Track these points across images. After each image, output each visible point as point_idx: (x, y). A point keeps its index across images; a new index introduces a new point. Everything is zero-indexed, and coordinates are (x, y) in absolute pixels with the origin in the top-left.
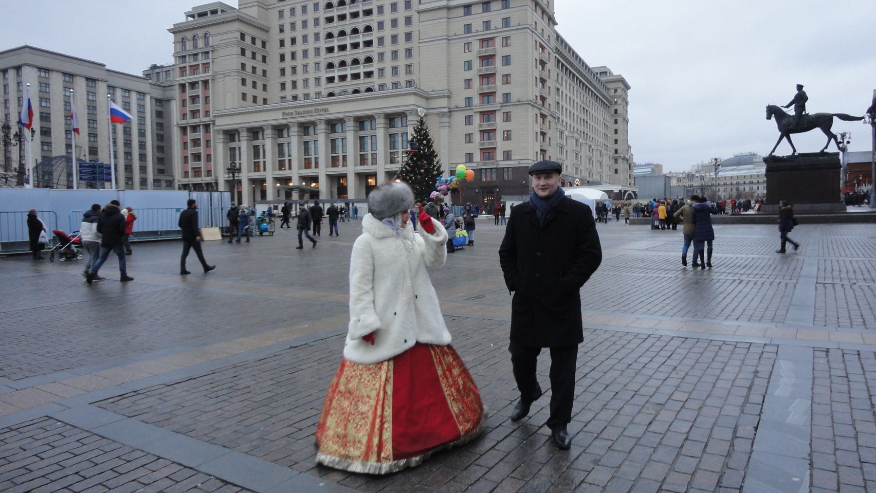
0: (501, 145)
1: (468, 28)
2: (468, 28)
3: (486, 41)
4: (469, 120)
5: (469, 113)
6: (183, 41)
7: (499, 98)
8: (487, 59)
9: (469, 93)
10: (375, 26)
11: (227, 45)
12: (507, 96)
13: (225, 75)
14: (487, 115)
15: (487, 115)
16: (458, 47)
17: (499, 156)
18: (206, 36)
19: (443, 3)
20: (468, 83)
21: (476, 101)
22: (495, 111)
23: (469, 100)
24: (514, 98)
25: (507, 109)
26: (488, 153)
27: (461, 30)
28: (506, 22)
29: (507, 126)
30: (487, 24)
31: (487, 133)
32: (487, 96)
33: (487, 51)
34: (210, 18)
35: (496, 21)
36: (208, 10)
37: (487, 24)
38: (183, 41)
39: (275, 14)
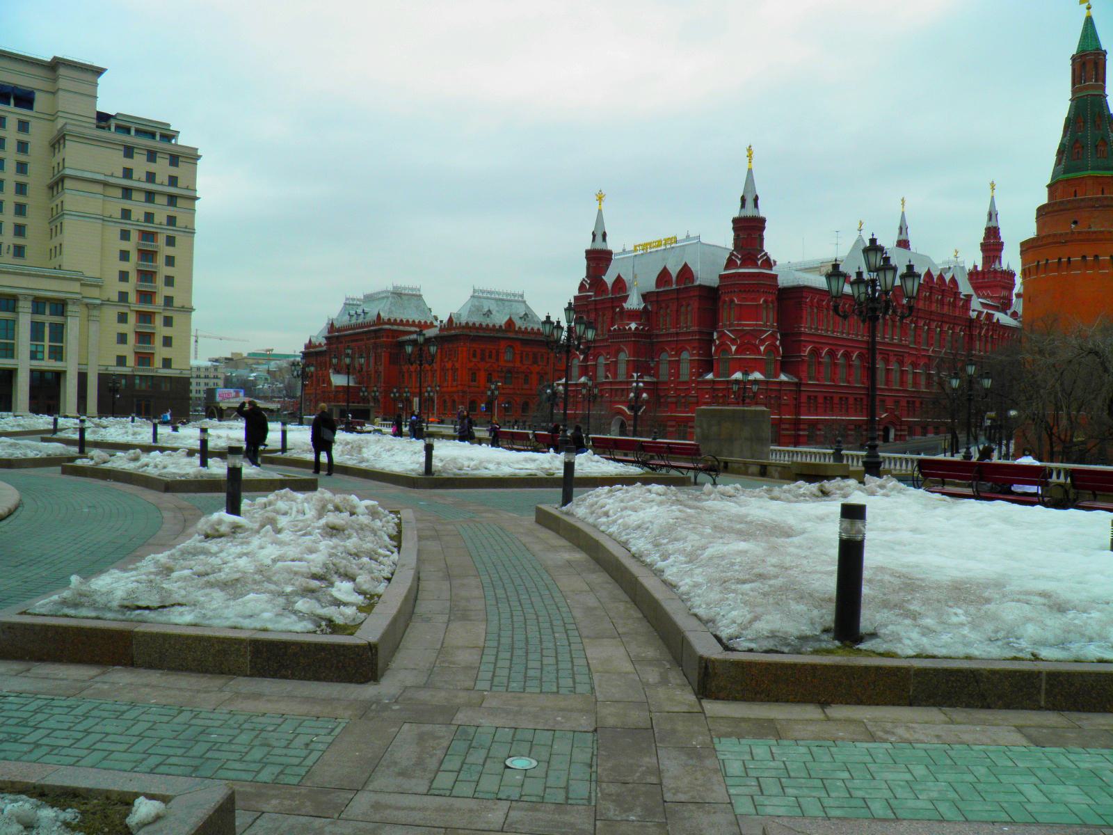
0: (160, 352)
1: (126, 214)
2: (126, 214)
3: (148, 236)
4: (122, 318)
5: (124, 310)
7: (160, 300)
8: (148, 255)
9: (124, 287)
12: (169, 301)
14: (146, 317)
15: (146, 317)
16: (115, 232)
17: (158, 362)
19: (101, 177)
20: (124, 276)
21: (132, 298)
22: (154, 313)
23: (123, 296)
24: (177, 303)
25: (168, 314)
26: (144, 358)
27: (118, 214)
28: (171, 220)
30: (149, 217)
31: (144, 337)
32: (146, 296)
35: (161, 215)
37: (149, 217)
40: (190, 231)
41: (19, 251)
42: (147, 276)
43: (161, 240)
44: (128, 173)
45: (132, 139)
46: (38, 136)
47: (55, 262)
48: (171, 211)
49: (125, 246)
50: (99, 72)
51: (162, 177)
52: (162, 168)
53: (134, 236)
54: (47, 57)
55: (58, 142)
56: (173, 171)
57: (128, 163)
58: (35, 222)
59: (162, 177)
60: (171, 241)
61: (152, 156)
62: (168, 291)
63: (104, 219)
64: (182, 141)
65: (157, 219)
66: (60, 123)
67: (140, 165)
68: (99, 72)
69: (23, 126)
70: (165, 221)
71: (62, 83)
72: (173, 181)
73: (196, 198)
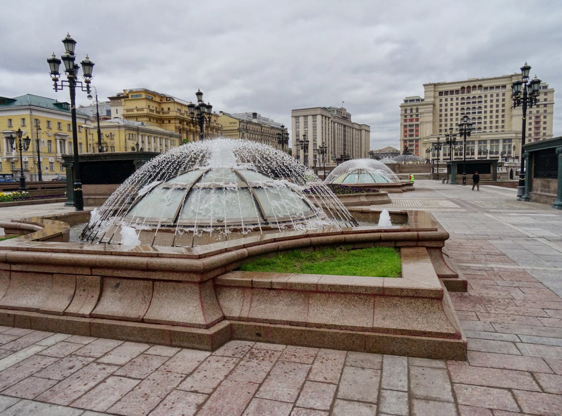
3: (537, 117)
6: (406, 110)
11: (428, 112)
12: (544, 134)
13: (427, 123)
18: (417, 109)
21: (533, 135)
24: (547, 134)
30: (538, 112)
33: (538, 120)
34: (420, 103)
38: (406, 110)
39: (438, 100)
40: (552, 113)
41: (503, 127)
42: (537, 128)
43: (542, 117)
48: (545, 109)
53: (533, 118)
56: (545, 97)
58: (506, 118)
60: (545, 117)
62: (545, 131)
64: (549, 87)
69: (504, 95)
70: (543, 112)
73: (553, 103)
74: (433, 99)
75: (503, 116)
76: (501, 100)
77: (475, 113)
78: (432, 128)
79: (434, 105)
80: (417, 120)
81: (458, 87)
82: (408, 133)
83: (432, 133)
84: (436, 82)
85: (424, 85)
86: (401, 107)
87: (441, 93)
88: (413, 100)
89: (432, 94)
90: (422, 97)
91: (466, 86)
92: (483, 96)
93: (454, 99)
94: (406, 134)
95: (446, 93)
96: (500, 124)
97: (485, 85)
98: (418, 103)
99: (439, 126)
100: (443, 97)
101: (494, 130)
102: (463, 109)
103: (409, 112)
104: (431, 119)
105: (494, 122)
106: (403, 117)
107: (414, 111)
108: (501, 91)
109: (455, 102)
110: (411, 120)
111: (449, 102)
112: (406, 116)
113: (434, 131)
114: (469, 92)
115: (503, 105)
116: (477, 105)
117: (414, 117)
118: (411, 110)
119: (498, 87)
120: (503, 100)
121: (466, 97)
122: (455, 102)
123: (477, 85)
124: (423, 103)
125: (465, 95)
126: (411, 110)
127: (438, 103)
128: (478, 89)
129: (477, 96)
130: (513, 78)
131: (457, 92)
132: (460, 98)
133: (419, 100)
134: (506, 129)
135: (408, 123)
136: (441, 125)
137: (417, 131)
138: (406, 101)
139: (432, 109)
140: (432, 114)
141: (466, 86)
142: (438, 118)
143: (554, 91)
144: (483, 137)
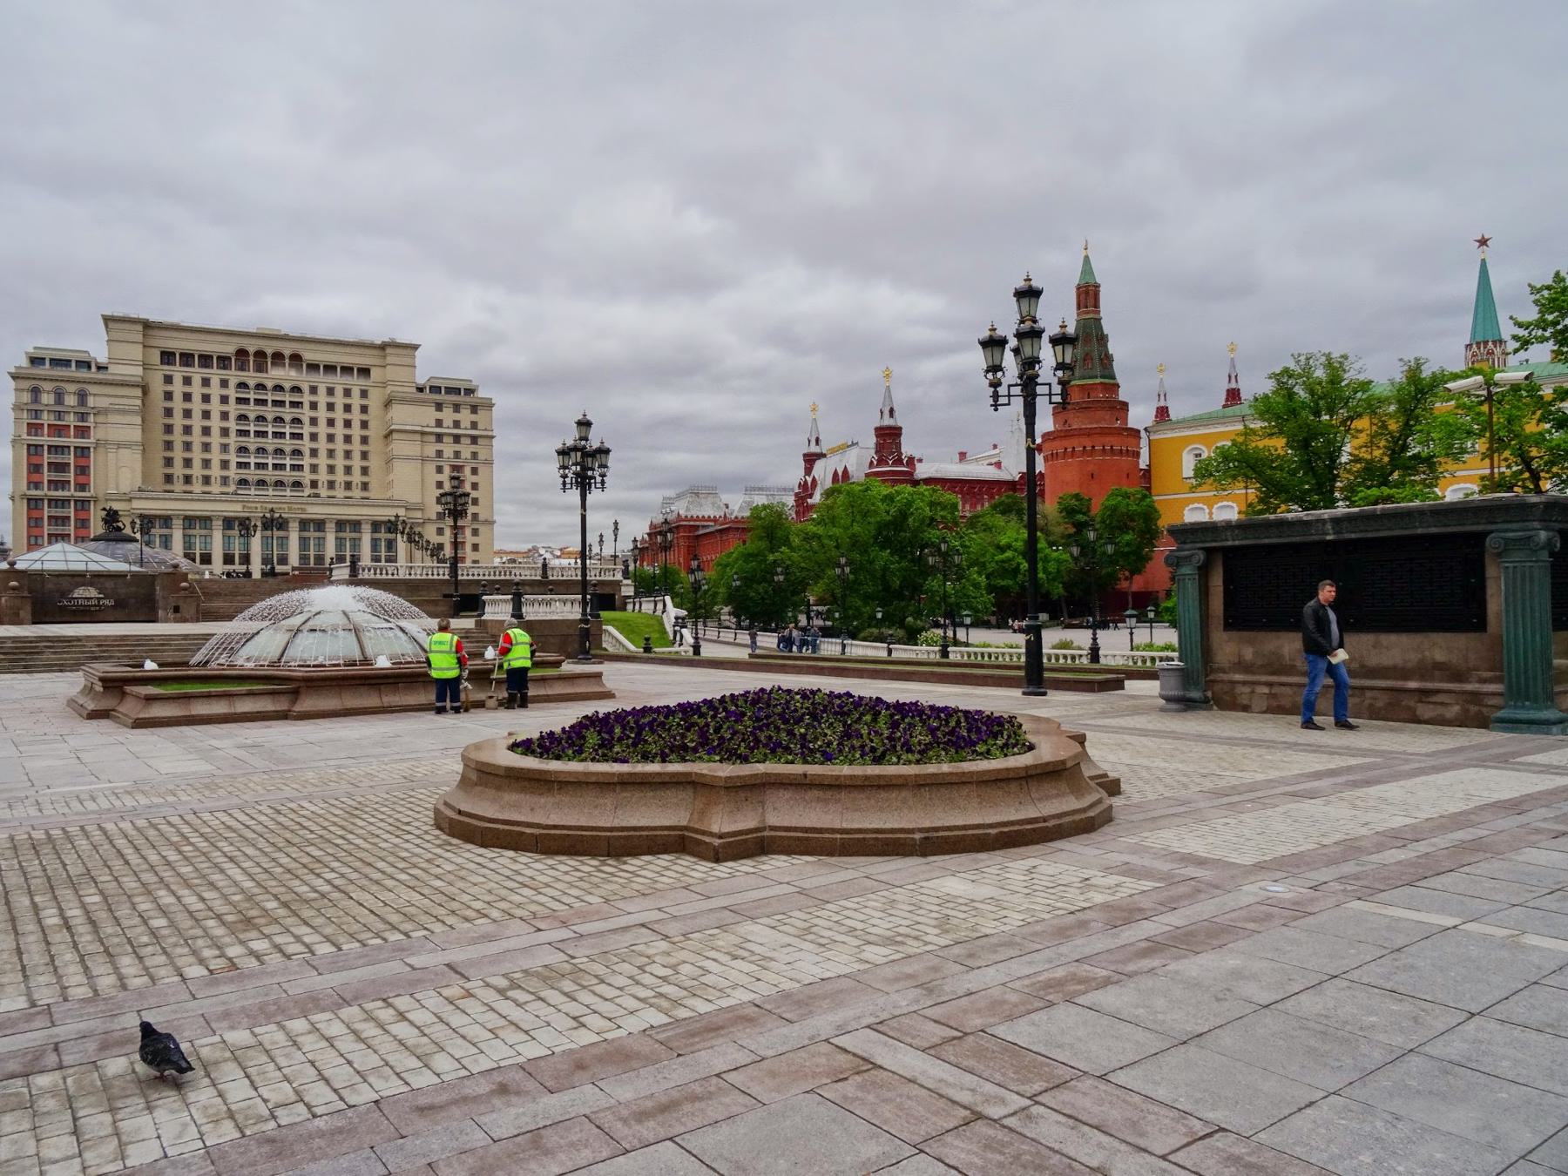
1: (439, 453)
2: (439, 453)
3: (456, 468)
6: (36, 391)
10: (306, 420)
12: (475, 516)
13: (119, 446)
16: (431, 468)
18: (82, 397)
24: (481, 517)
28: (475, 455)
29: (476, 540)
30: (457, 454)
34: (93, 374)
36: (74, 357)
37: (457, 454)
38: (36, 391)
41: (365, 486)
43: (467, 471)
44: (439, 423)
45: (442, 397)
46: (375, 401)
47: (389, 494)
48: (474, 448)
49: (440, 477)
50: (415, 347)
51: (465, 423)
52: (465, 416)
53: (447, 470)
54: (378, 342)
55: (388, 404)
56: (474, 417)
57: (439, 415)
58: (374, 463)
59: (465, 423)
60: (474, 471)
61: (457, 408)
63: (424, 459)
64: (482, 393)
65: (463, 456)
66: (389, 389)
67: (448, 415)
68: (415, 347)
69: (364, 394)
71: (389, 360)
72: (474, 425)
74: (139, 371)
75: (364, 455)
76: (356, 409)
77: (281, 435)
78: (138, 466)
79: (145, 390)
80: (83, 432)
81: (229, 348)
82: (46, 475)
83: (139, 483)
84: (153, 317)
85: (107, 320)
86: (15, 377)
87: (167, 357)
88: (65, 363)
89: (136, 352)
90: (100, 353)
91: (251, 350)
92: (305, 388)
93: (215, 381)
94: (35, 477)
95: (187, 359)
96: (357, 478)
97: (309, 355)
98: (83, 374)
99: (162, 462)
100: (178, 372)
101: (340, 493)
102: (242, 418)
103: (47, 399)
104: (136, 435)
105: (340, 470)
106: (25, 415)
107: (71, 400)
108: (355, 382)
109: (215, 391)
110: (59, 430)
111: (197, 390)
112: (37, 413)
113: (146, 476)
114: (260, 368)
115: (364, 425)
116: (288, 413)
117: (71, 420)
118: (59, 396)
119: (347, 370)
120: (364, 409)
121: (252, 383)
122: (215, 391)
123: (287, 353)
124: (101, 376)
125: (251, 377)
126: (59, 396)
127: (158, 387)
128: (291, 365)
129: (287, 386)
130: (389, 350)
131: (224, 361)
132: (233, 382)
133: (88, 365)
134: (373, 493)
135: (45, 439)
136: (169, 462)
137: (83, 470)
138: (35, 361)
139: (139, 402)
140: (138, 420)
141: (251, 350)
142: (159, 436)
143: (492, 405)
144: (316, 511)
